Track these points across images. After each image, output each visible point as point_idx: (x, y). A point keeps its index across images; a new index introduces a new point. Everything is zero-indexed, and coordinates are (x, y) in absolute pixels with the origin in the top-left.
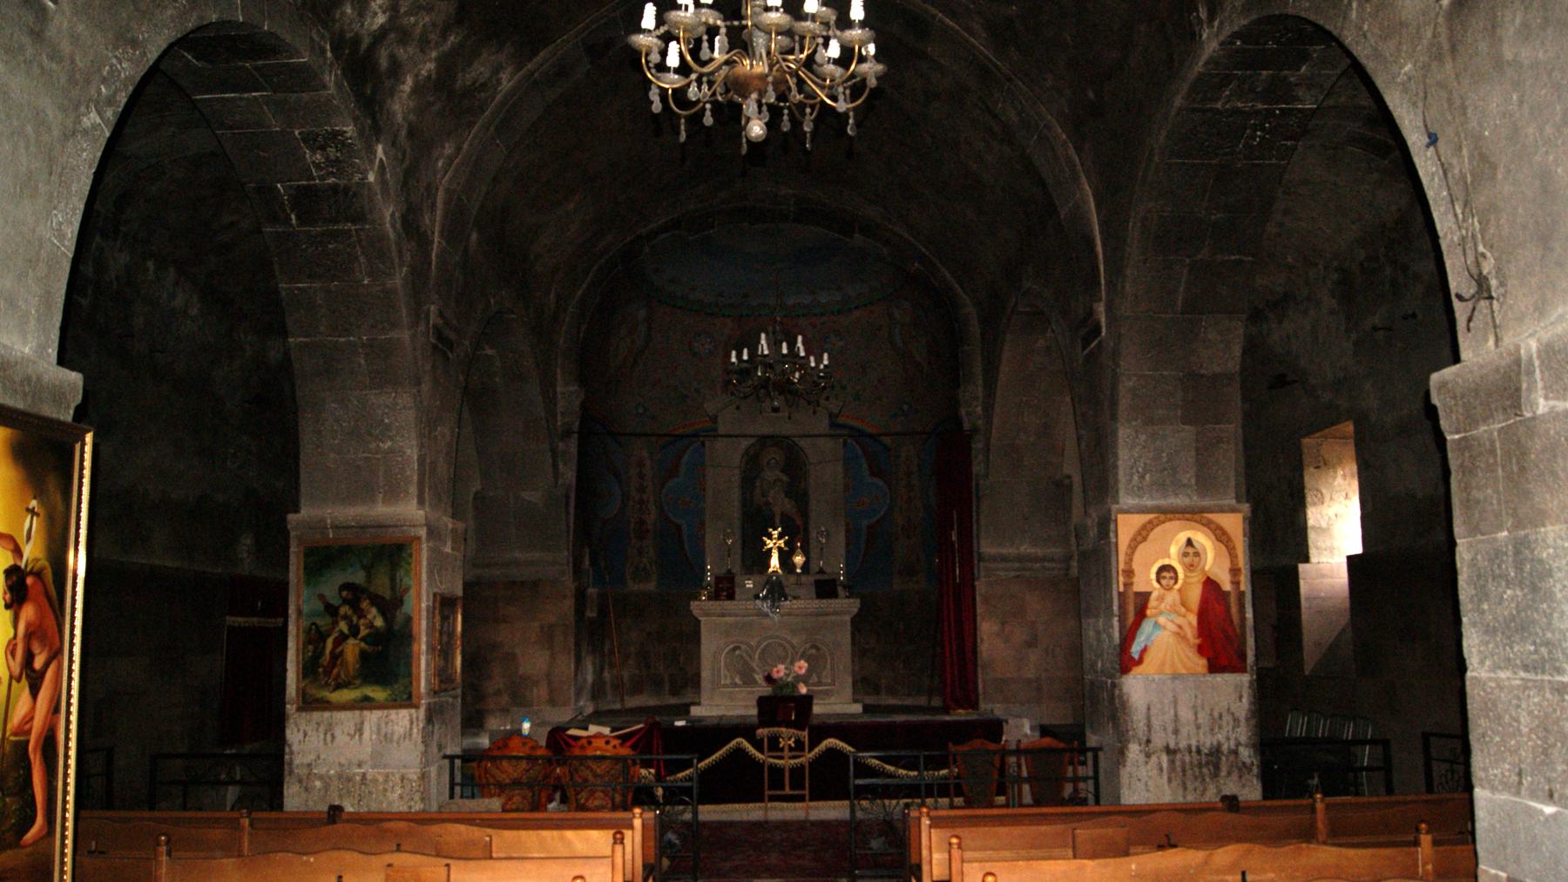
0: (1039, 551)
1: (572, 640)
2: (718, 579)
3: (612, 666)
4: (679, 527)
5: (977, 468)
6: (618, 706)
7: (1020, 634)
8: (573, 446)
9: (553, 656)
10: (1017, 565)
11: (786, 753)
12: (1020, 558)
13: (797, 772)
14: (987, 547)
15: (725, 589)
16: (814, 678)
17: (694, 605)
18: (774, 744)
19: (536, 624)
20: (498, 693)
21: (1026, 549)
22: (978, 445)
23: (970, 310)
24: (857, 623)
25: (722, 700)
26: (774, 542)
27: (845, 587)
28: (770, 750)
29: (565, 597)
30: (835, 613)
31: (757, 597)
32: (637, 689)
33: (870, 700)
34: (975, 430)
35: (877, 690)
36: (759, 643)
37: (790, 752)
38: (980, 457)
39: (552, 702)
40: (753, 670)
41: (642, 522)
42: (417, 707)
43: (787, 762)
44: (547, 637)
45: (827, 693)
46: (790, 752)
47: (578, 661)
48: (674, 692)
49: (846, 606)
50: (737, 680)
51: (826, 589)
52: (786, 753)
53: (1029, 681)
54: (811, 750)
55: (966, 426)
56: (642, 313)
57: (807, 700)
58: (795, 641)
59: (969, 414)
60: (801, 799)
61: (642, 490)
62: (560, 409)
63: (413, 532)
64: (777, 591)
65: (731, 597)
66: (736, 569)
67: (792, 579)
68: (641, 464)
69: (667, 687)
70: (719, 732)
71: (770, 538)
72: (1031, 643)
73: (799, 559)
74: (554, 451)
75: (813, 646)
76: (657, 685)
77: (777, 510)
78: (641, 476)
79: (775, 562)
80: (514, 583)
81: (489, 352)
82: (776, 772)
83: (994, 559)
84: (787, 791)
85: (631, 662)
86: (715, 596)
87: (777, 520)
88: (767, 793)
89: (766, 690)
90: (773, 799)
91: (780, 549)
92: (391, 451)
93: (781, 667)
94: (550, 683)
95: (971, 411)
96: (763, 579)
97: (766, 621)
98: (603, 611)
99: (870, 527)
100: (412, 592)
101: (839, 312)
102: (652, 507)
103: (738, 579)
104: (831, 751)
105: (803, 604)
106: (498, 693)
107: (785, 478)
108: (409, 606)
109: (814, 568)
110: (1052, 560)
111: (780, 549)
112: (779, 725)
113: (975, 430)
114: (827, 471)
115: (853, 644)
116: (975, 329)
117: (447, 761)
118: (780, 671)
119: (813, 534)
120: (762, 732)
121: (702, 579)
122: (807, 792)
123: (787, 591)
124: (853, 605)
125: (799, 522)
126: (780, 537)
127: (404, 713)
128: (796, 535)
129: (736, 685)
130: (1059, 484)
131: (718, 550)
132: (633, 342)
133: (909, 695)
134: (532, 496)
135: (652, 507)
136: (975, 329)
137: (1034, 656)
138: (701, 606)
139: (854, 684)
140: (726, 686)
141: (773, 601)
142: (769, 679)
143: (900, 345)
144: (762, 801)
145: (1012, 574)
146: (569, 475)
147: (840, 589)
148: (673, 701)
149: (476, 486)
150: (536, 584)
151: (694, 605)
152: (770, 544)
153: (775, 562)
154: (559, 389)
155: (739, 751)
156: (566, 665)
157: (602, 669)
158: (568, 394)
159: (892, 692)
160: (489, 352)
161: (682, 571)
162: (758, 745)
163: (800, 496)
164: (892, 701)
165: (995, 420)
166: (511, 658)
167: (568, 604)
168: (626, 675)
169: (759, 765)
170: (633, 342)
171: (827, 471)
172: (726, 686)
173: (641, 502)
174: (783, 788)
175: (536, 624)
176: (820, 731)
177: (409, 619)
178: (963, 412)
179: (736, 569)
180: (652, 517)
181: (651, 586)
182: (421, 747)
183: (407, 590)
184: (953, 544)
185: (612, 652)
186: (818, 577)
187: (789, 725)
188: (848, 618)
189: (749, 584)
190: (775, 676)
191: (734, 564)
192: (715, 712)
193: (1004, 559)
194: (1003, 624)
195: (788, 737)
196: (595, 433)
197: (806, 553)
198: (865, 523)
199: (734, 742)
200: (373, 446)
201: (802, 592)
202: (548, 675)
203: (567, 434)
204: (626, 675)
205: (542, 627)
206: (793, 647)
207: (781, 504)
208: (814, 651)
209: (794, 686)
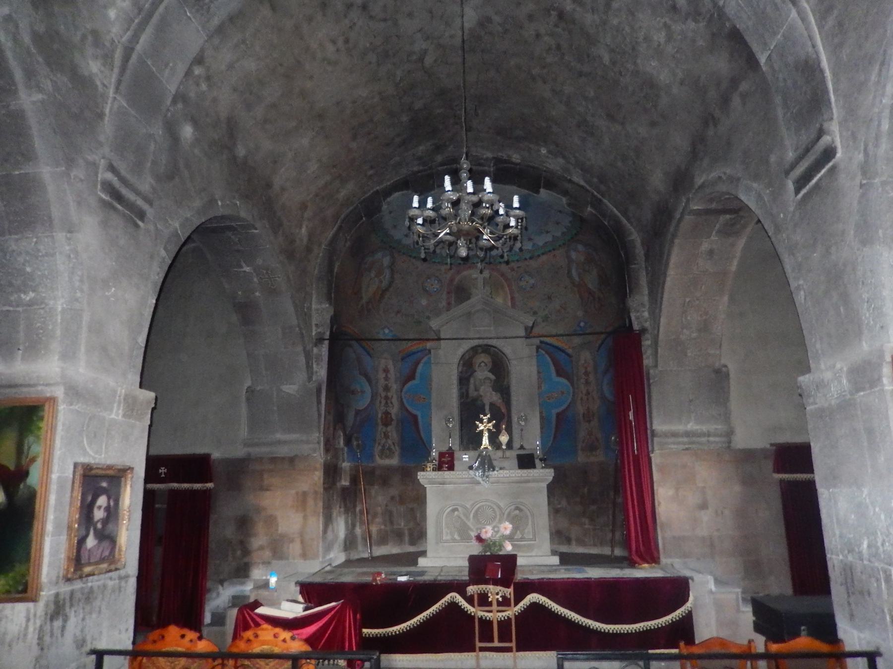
0: (704, 428)
1: (321, 504)
2: (441, 455)
3: (362, 523)
4: (415, 417)
5: (647, 361)
6: (366, 555)
7: (693, 499)
8: (325, 348)
9: (305, 518)
10: (685, 440)
11: (495, 607)
12: (687, 434)
13: (504, 625)
14: (659, 424)
15: (447, 462)
16: (518, 535)
17: (421, 476)
18: (483, 600)
19: (293, 492)
20: (261, 548)
21: (691, 426)
22: (646, 343)
23: (635, 237)
24: (551, 488)
25: (443, 556)
26: (484, 426)
27: (541, 460)
28: (480, 605)
29: (316, 469)
30: (534, 481)
31: (471, 468)
32: (383, 540)
33: (564, 549)
34: (644, 331)
35: (568, 541)
36: (473, 505)
37: (498, 607)
38: (649, 352)
39: (304, 556)
40: (469, 528)
41: (387, 413)
42: (34, 600)
43: (495, 615)
44: (302, 500)
45: (530, 548)
46: (498, 607)
47: (328, 520)
48: (412, 543)
49: (543, 475)
50: (456, 537)
51: (526, 461)
52: (495, 607)
53: (703, 539)
54: (516, 604)
55: (636, 327)
56: (386, 261)
57: (510, 561)
58: (502, 505)
59: (637, 318)
60: (509, 650)
61: (387, 388)
62: (314, 322)
63: (48, 392)
64: (487, 464)
65: (451, 468)
66: (456, 447)
67: (499, 453)
68: (386, 371)
69: (407, 539)
70: (431, 591)
71: (481, 421)
72: (703, 506)
73: (504, 438)
74: (308, 355)
75: (517, 508)
76: (399, 536)
77: (487, 402)
78: (386, 379)
79: (485, 441)
80: (275, 458)
81: (247, 269)
82: (486, 624)
83: (666, 435)
84: (496, 644)
85: (377, 520)
86: (439, 468)
87: (487, 408)
88: (479, 644)
89: (476, 549)
90: (482, 649)
91: (489, 430)
92: (31, 303)
93: (489, 528)
94: (302, 542)
95: (640, 316)
96: (476, 453)
97: (477, 488)
98: (354, 480)
99: (558, 415)
100: (39, 462)
101: (531, 258)
102: (395, 401)
103: (456, 455)
104: (534, 605)
105: (508, 473)
106: (261, 548)
107: (493, 377)
108: (34, 478)
109: (516, 445)
110: (715, 435)
111: (489, 430)
112: (486, 582)
113: (644, 331)
114: (524, 368)
115: (549, 504)
116: (639, 251)
117: (94, 657)
118: (488, 533)
119: (515, 419)
120: (471, 589)
121: (429, 453)
122: (513, 644)
123: (495, 463)
124: (548, 475)
125: (504, 410)
126: (489, 421)
127: (21, 607)
128: (502, 418)
129: (454, 540)
130: (718, 372)
131: (442, 434)
132: (381, 282)
133: (595, 545)
134: (290, 389)
135: (395, 401)
136: (639, 251)
137: (705, 517)
138: (427, 477)
139: (551, 534)
140: (446, 541)
141: (484, 471)
142: (479, 539)
143: (577, 279)
144: (473, 650)
145: (682, 447)
146: (321, 372)
147: (537, 462)
148: (412, 549)
149: (248, 383)
150: (292, 460)
151: (421, 476)
152: (481, 427)
153: (485, 441)
154: (313, 306)
155: (453, 605)
156: (316, 524)
157: (354, 526)
158: (321, 312)
159: (580, 542)
160: (247, 269)
161: (415, 449)
162: (470, 600)
163: (502, 388)
164: (581, 550)
165: (663, 321)
166: (271, 521)
167: (318, 476)
168: (374, 529)
169: (471, 618)
170: (381, 282)
171: (524, 368)
172: (446, 541)
173: (387, 398)
174: (492, 641)
175: (293, 492)
176: (523, 589)
177: (32, 496)
178: (633, 316)
179: (456, 447)
180: (394, 411)
181: (394, 461)
182: (35, 650)
183: (33, 460)
184: (631, 422)
185: (362, 512)
186: (522, 452)
187: (496, 582)
188: (544, 485)
189: (466, 458)
190: (484, 536)
191: (453, 443)
192: (439, 563)
193: (674, 435)
194: (677, 489)
195: (495, 592)
196: (340, 341)
197: (509, 431)
198: (554, 412)
199: (448, 598)
200: (13, 298)
201: (506, 464)
202: (302, 535)
203: (320, 340)
204: (374, 529)
205: (297, 493)
206: (499, 507)
207: (490, 396)
208: (517, 512)
209: (501, 546)
